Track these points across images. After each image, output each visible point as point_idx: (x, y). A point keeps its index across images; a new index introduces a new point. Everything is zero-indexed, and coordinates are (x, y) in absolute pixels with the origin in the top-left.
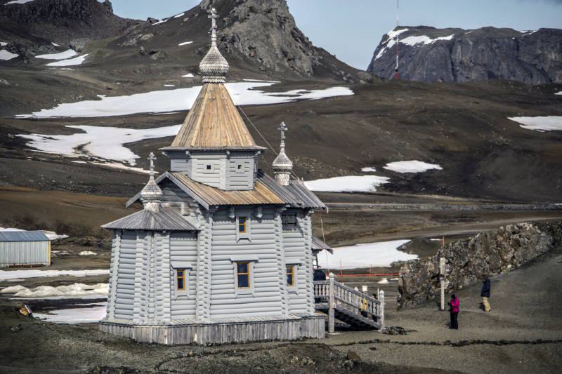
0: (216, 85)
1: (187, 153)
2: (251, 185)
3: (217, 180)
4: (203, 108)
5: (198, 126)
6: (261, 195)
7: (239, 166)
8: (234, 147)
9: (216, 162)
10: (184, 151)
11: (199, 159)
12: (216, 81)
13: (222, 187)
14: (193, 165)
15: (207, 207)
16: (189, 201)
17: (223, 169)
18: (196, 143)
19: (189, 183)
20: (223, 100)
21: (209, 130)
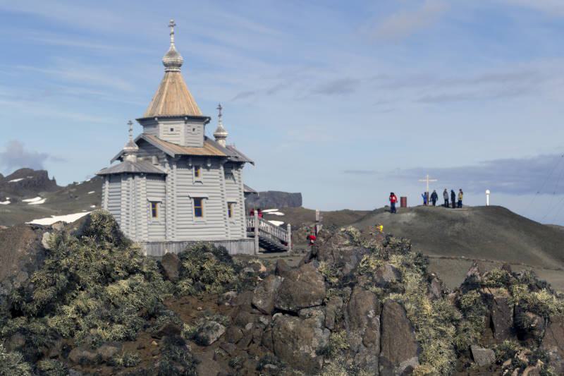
1: (156, 119)
2: (202, 144)
3: (177, 139)
4: (166, 88)
5: (163, 101)
6: (208, 150)
7: (194, 130)
8: (190, 114)
9: (177, 126)
10: (154, 118)
11: (164, 124)
12: (175, 70)
13: (182, 144)
14: (160, 128)
15: (173, 156)
16: (158, 154)
17: (182, 131)
18: (162, 113)
19: (158, 141)
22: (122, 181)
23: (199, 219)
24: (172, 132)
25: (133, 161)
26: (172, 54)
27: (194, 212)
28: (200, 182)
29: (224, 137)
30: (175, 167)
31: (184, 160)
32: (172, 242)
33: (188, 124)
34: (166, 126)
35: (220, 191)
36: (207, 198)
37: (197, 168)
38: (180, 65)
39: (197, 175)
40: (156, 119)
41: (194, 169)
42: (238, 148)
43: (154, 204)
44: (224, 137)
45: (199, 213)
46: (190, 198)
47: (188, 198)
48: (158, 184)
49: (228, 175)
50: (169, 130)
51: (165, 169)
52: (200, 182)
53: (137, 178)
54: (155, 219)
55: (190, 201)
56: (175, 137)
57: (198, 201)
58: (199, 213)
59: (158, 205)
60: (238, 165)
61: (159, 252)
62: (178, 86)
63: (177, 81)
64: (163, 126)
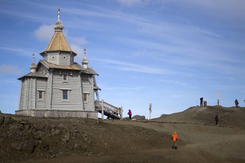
0: (58, 32)
7: (64, 58)
11: (50, 55)
12: (59, 30)
20: (60, 37)
21: (54, 46)
22: (25, 81)
23: (66, 100)
24: (53, 59)
25: (33, 72)
26: (58, 23)
27: (62, 96)
28: (67, 82)
29: (86, 64)
30: (52, 74)
31: (56, 71)
32: (47, 110)
33: (61, 55)
34: (51, 56)
35: (78, 88)
36: (70, 90)
37: (65, 76)
38: (62, 29)
39: (65, 79)
40: (46, 52)
41: (63, 76)
42: (94, 69)
43: (41, 92)
44: (86, 64)
45: (65, 97)
46: (61, 90)
47: (60, 90)
48: (43, 83)
49: (82, 80)
50: (52, 58)
51: (47, 75)
52: (67, 82)
53: (31, 79)
54: (40, 99)
55: (60, 91)
56: (56, 61)
57: (65, 91)
58: (65, 97)
59: (43, 93)
60: (91, 75)
61: (41, 115)
62: (59, 37)
63: (58, 36)
64: (49, 57)
